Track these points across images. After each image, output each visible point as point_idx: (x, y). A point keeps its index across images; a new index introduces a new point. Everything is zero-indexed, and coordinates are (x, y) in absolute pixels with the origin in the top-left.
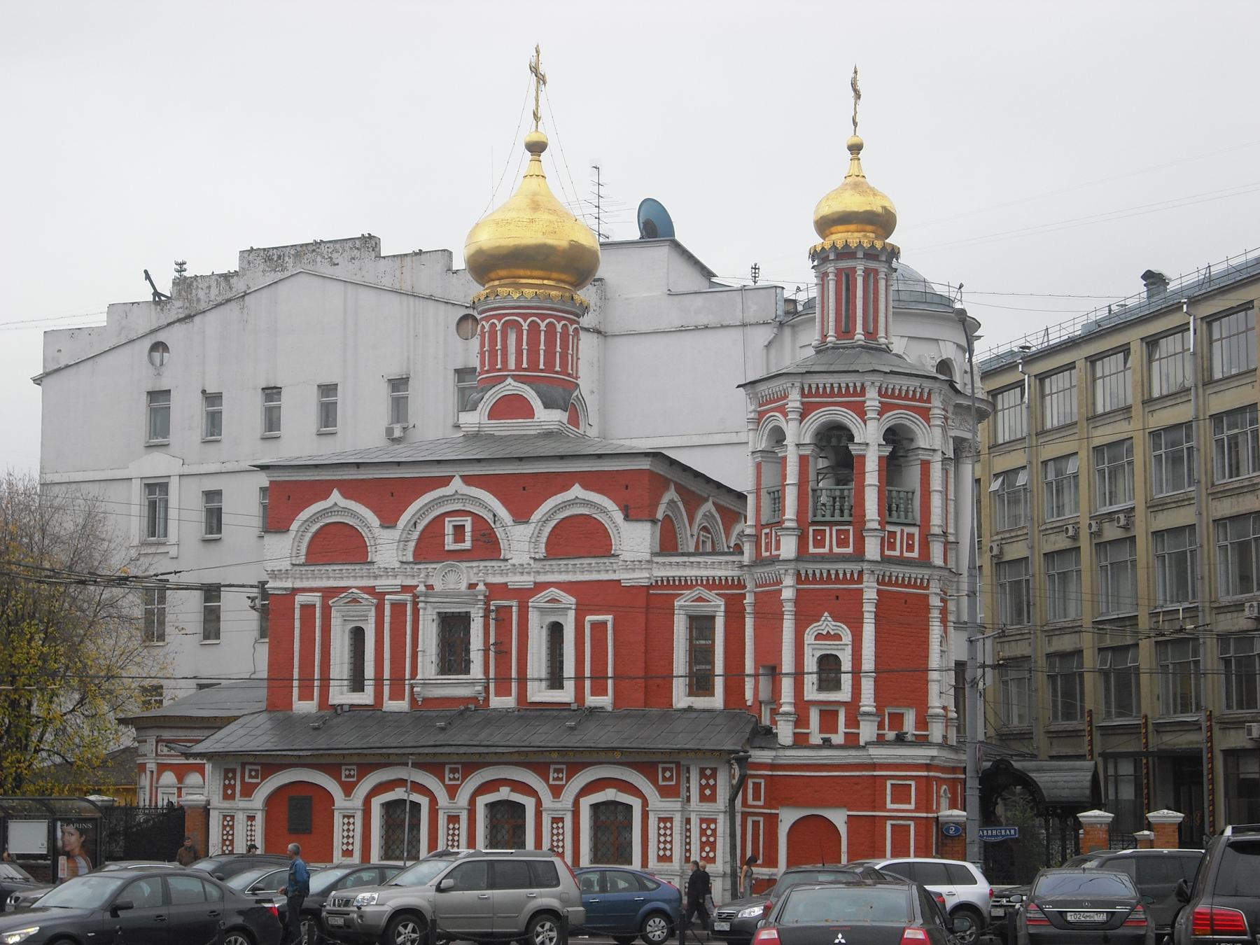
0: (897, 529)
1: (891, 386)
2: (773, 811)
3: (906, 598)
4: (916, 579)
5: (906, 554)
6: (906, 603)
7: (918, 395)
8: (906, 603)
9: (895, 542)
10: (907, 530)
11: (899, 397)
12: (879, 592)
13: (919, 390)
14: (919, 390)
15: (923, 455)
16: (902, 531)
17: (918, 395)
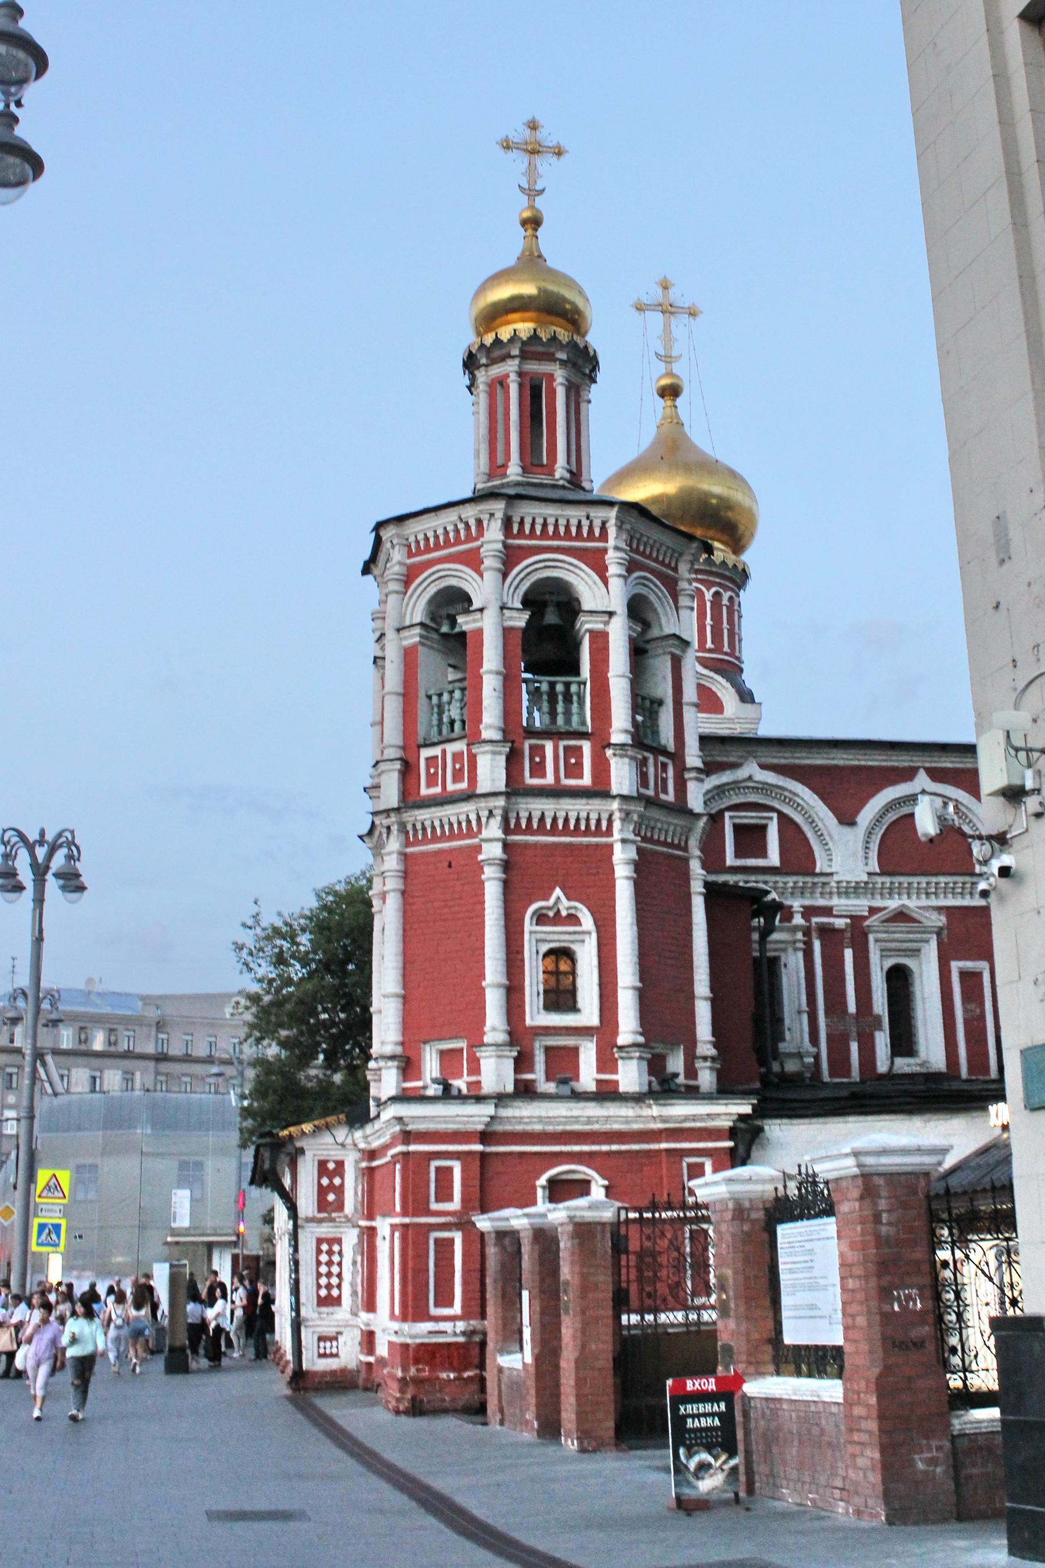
0: (436, 751)
1: (421, 537)
2: (373, 1224)
3: (449, 859)
4: (459, 823)
5: (451, 787)
6: (450, 866)
7: (462, 533)
8: (450, 866)
9: (436, 773)
10: (451, 748)
11: (438, 547)
12: (405, 857)
13: (461, 526)
14: (461, 526)
15: (466, 623)
16: (444, 752)
17: (462, 533)
